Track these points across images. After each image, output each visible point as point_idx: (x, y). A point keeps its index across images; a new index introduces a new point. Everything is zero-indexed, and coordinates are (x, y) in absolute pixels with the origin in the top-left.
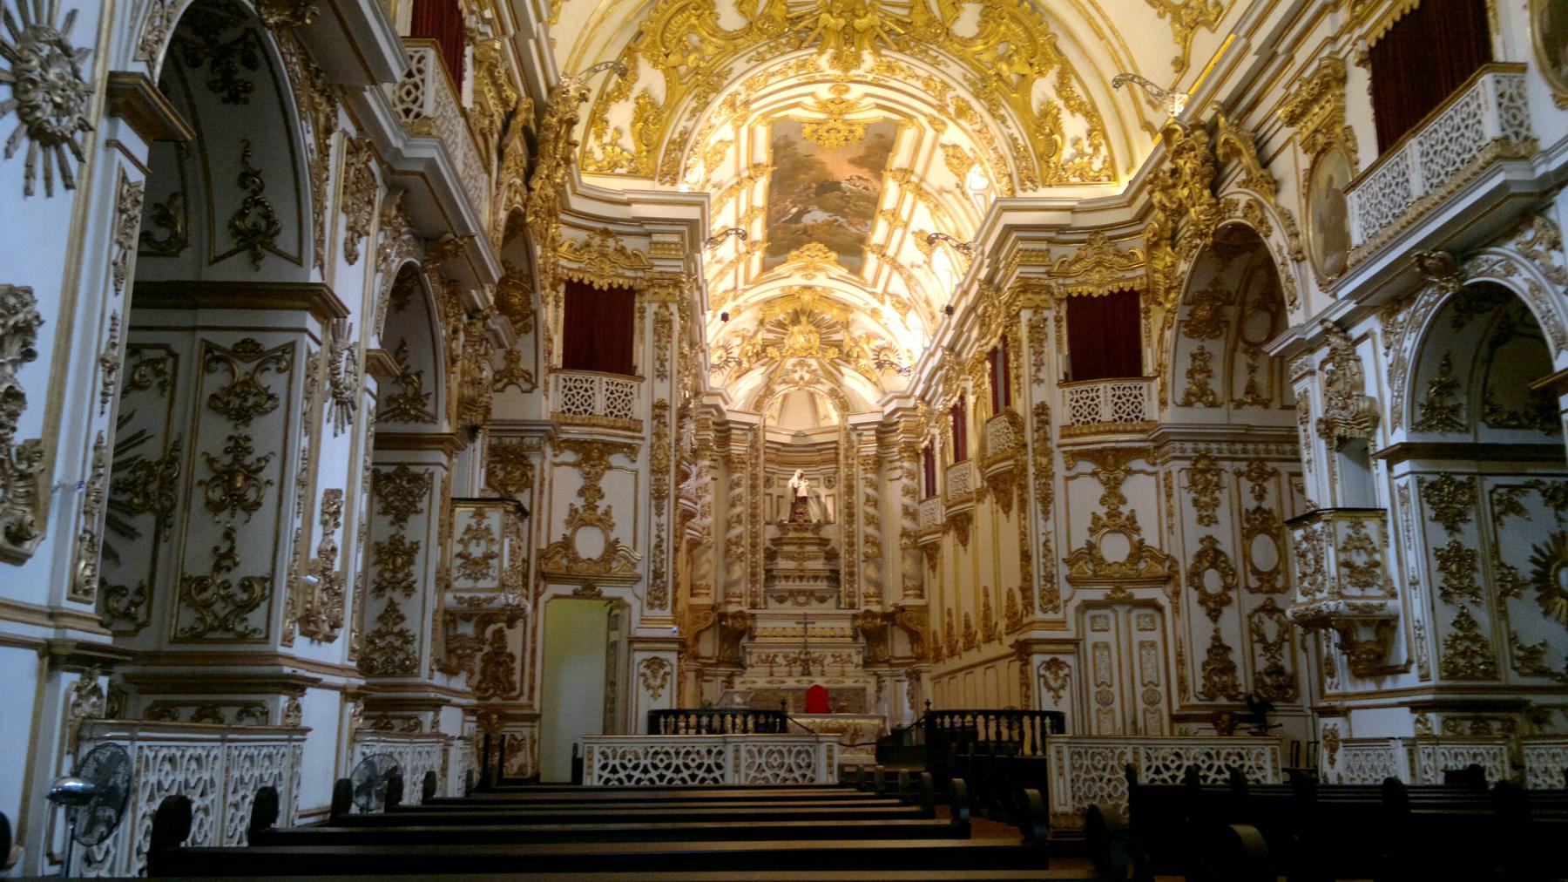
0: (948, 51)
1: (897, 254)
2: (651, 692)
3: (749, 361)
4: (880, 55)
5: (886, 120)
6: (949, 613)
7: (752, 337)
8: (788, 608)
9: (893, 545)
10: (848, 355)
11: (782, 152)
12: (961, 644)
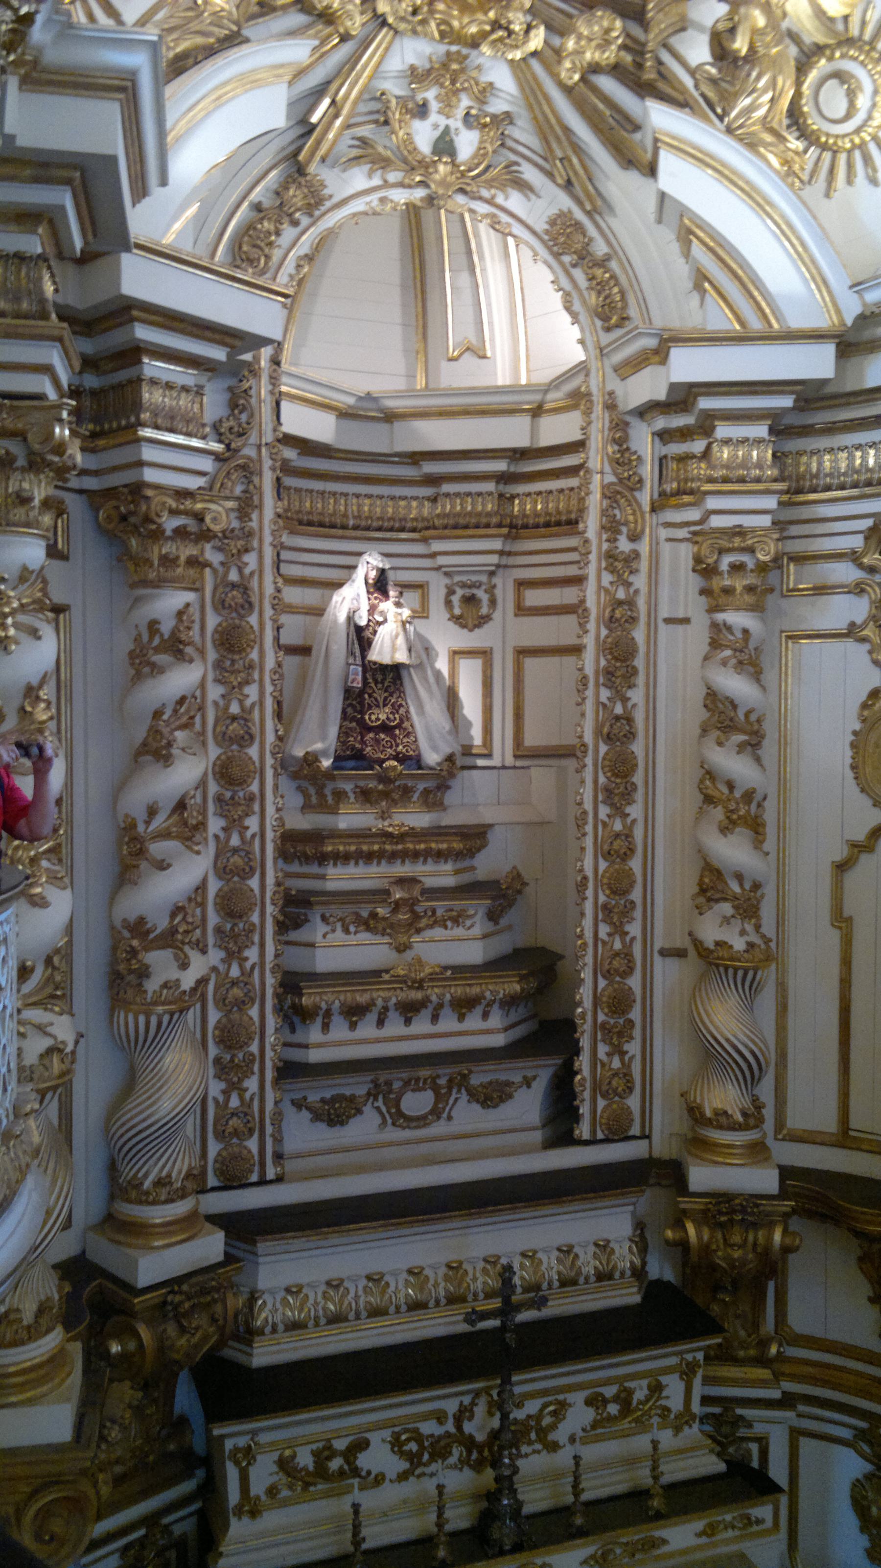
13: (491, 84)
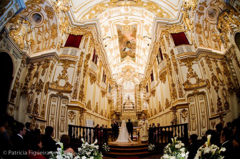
2: (71, 120)
6: (151, 109)
8: (127, 111)
9: (142, 100)
12: (154, 114)
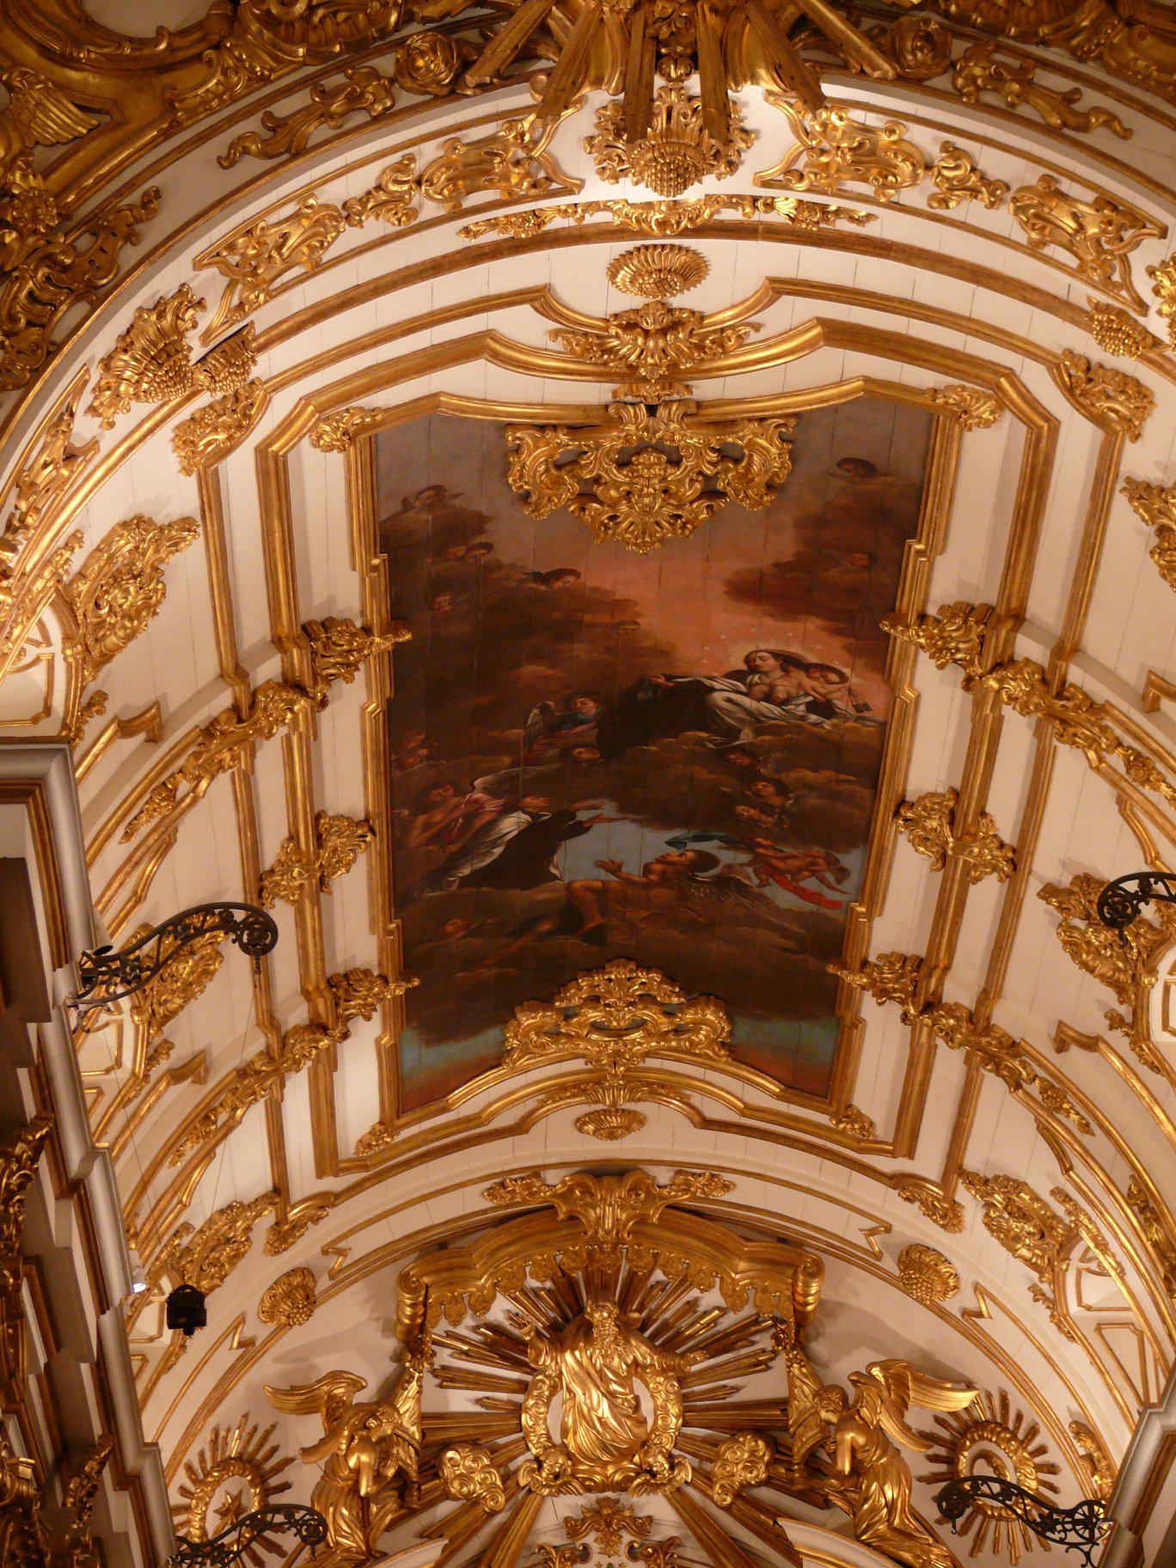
0: (1119, 71)
1: (990, 992)
3: (364, 1522)
4: (816, 101)
5: (875, 392)
7: (371, 1410)
10: (815, 1466)
11: (428, 566)
13: (650, 1519)
